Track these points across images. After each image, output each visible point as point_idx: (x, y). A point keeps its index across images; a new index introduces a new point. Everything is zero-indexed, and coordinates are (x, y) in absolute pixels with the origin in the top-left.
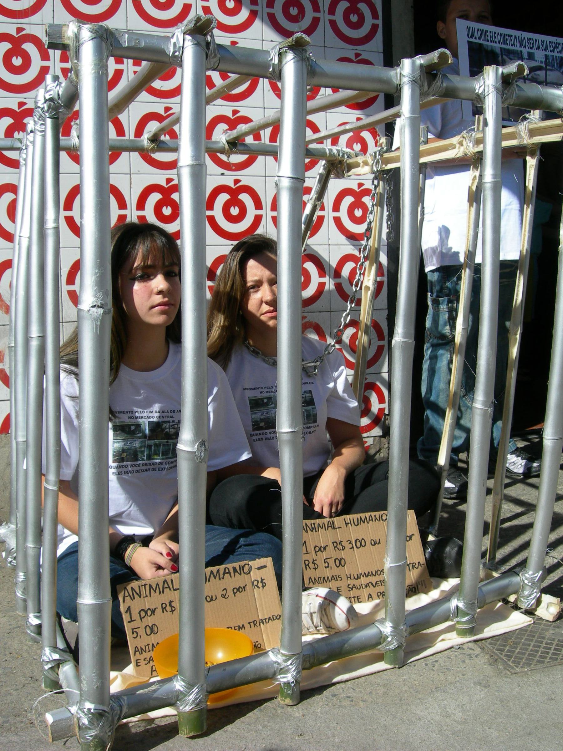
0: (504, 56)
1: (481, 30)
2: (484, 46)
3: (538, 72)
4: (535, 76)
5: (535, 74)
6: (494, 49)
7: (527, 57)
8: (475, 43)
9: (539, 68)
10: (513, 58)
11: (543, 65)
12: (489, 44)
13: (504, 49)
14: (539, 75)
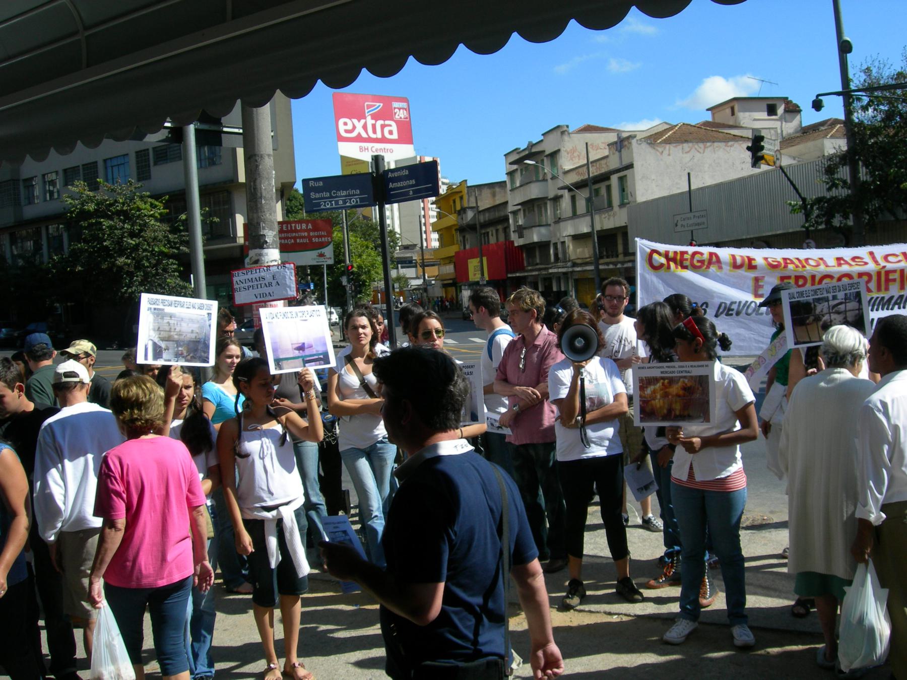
0: (816, 303)
3: (839, 307)
9: (841, 303)
11: (844, 301)
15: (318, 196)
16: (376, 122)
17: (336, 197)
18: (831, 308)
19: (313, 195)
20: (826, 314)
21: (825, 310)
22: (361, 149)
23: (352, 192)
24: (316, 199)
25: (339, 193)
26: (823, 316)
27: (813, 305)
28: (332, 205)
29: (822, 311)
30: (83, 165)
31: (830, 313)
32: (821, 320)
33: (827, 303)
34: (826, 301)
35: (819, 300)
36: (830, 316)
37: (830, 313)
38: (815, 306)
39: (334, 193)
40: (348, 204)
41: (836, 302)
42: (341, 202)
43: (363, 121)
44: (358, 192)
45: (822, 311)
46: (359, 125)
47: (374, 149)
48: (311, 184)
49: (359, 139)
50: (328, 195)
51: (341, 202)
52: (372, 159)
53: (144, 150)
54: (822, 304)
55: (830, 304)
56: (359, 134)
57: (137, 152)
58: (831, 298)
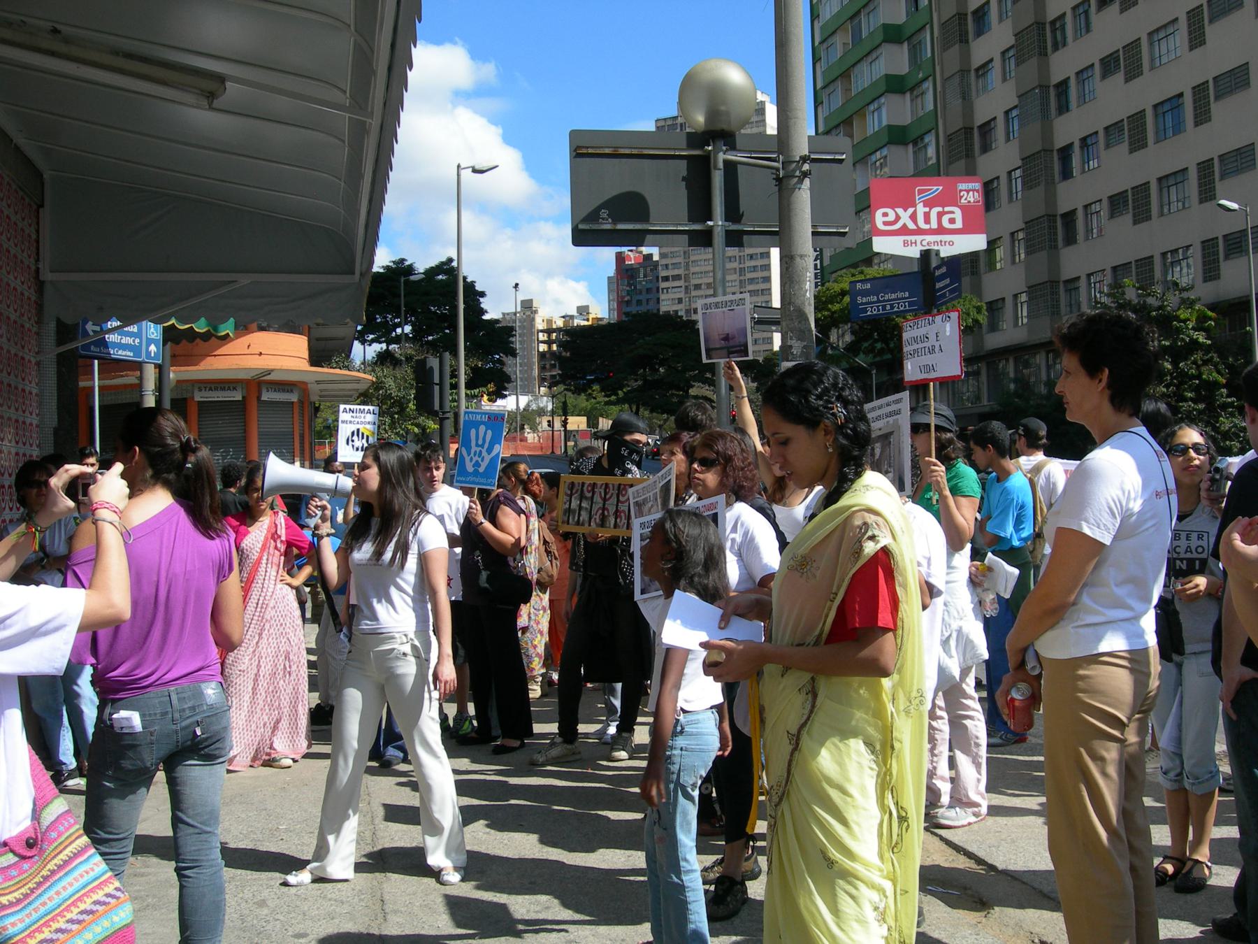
15: (865, 300)
19: (859, 300)
22: (905, 244)
23: (900, 295)
24: (862, 304)
30: (1136, 261)
43: (911, 210)
44: (907, 294)
46: (905, 216)
49: (904, 231)
53: (1213, 239)
56: (905, 225)
57: (1203, 242)
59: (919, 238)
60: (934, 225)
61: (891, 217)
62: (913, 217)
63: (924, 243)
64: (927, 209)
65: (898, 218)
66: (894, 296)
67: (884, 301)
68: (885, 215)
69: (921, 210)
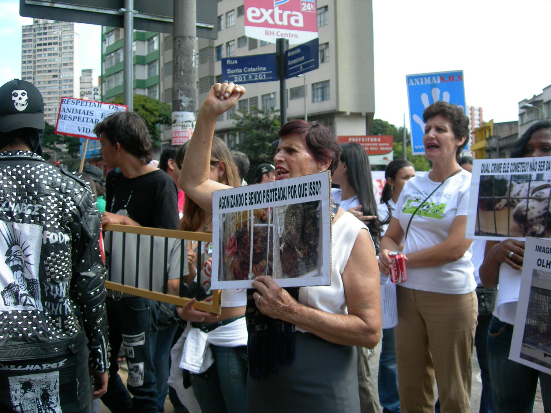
0: (513, 182)
1: (495, 164)
2: (496, 177)
4: (539, 194)
5: (540, 193)
6: (505, 177)
7: (535, 179)
8: (488, 176)
10: (521, 182)
12: (502, 174)
13: (515, 176)
14: (543, 193)
15: (233, 71)
16: (283, 12)
17: (248, 73)
18: (531, 191)
19: (229, 71)
20: (524, 198)
21: (523, 194)
22: (267, 33)
23: (259, 69)
24: (231, 74)
25: (250, 70)
26: (519, 201)
27: (508, 185)
28: (243, 79)
29: (518, 194)
31: (528, 198)
32: (514, 206)
33: (527, 184)
34: (527, 181)
35: (518, 179)
36: (528, 202)
37: (528, 198)
38: (511, 186)
39: (246, 70)
40: (256, 79)
41: (541, 183)
42: (250, 77)
43: (270, 11)
45: (518, 194)
47: (279, 34)
48: (229, 62)
49: (265, 24)
50: (241, 71)
51: (250, 77)
52: (277, 42)
54: (521, 185)
55: (531, 186)
58: (534, 177)
59: (275, 30)
60: (285, 23)
61: (258, 14)
62: (272, 16)
63: (279, 34)
64: (281, 12)
65: (262, 15)
66: (255, 69)
67: (248, 73)
68: (254, 12)
69: (277, 11)
